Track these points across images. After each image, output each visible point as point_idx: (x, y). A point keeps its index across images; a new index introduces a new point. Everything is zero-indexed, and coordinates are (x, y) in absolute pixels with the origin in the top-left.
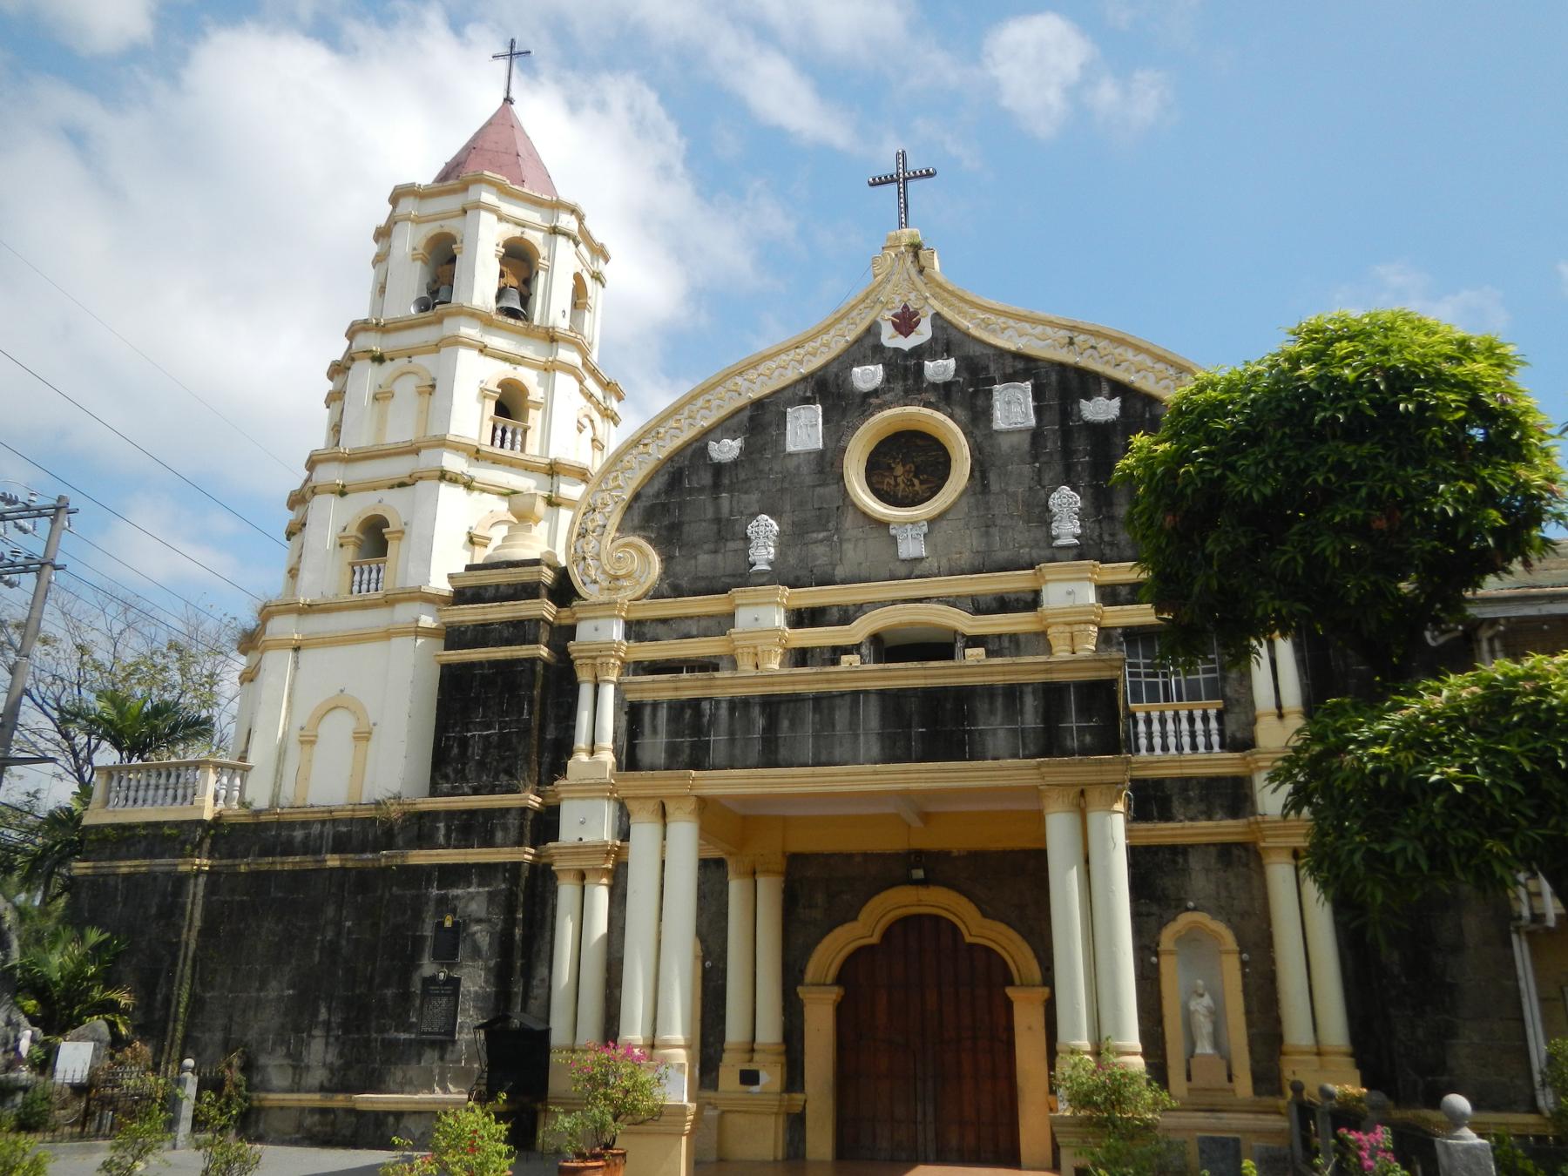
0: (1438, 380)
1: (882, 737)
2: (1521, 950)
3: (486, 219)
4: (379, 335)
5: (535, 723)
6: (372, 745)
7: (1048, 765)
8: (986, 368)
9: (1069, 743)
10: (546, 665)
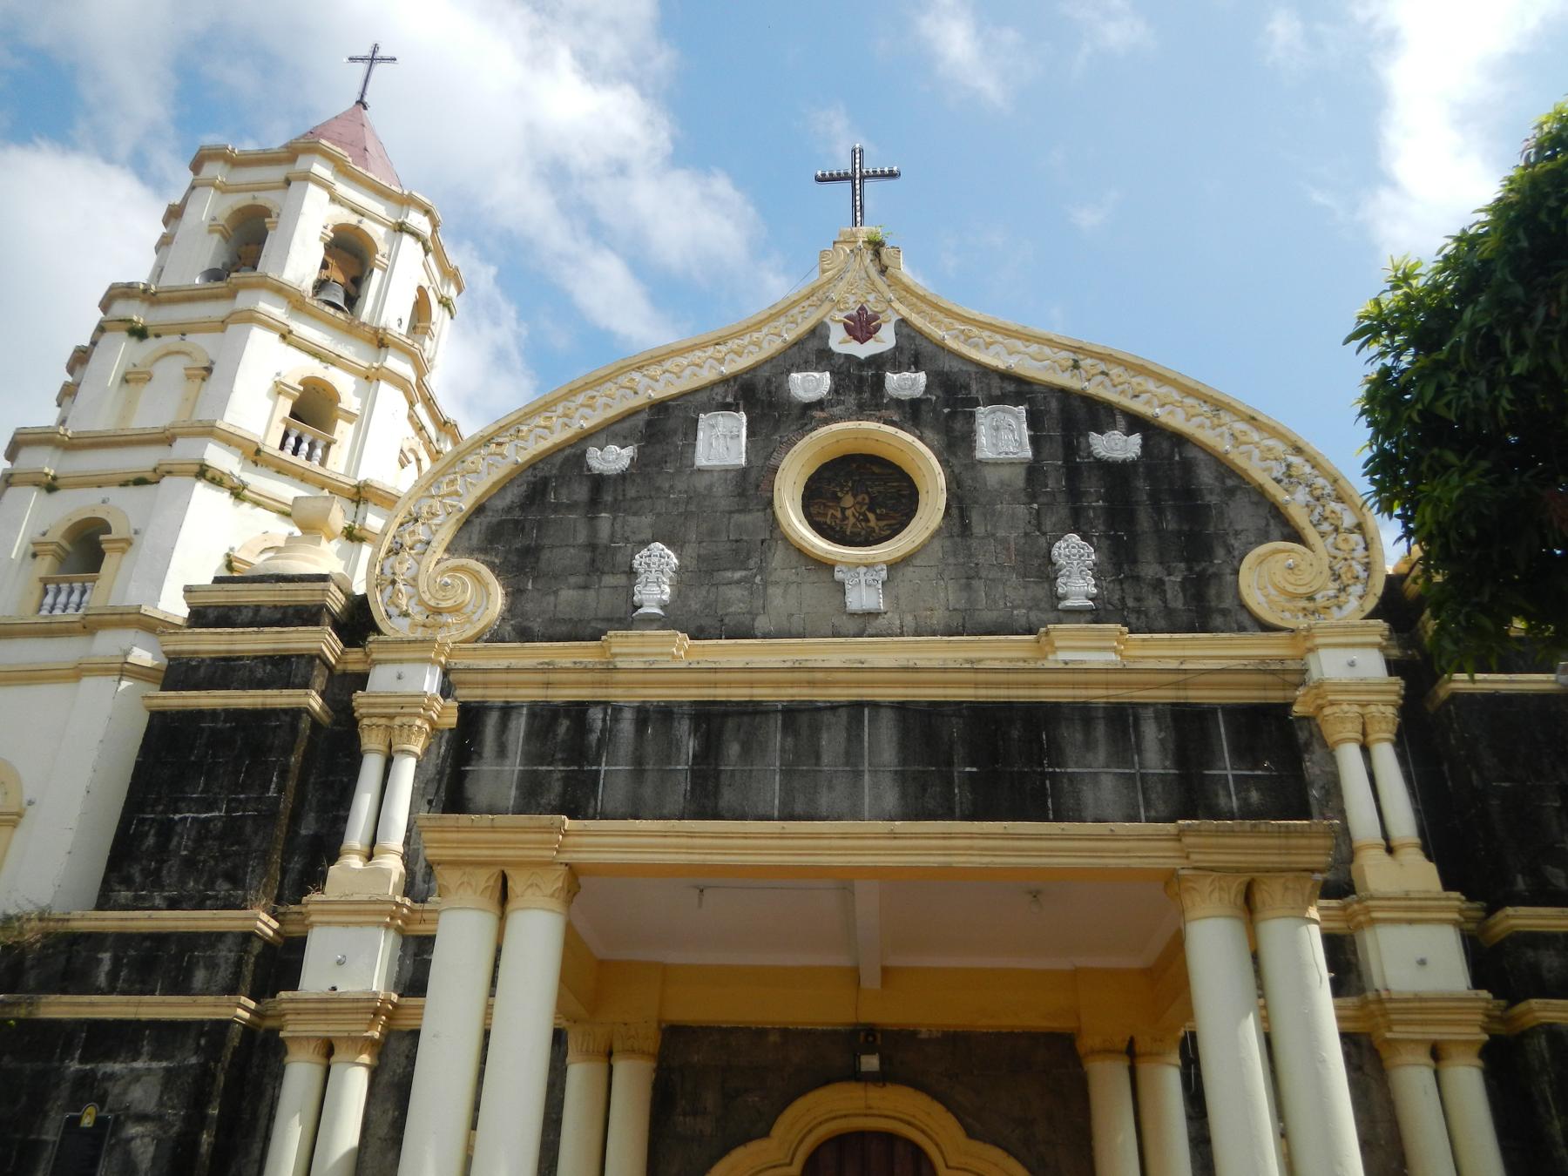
1: (902, 777)
5: (286, 805)
7: (1197, 832)
8: (967, 387)
9: (1222, 801)
10: (316, 724)
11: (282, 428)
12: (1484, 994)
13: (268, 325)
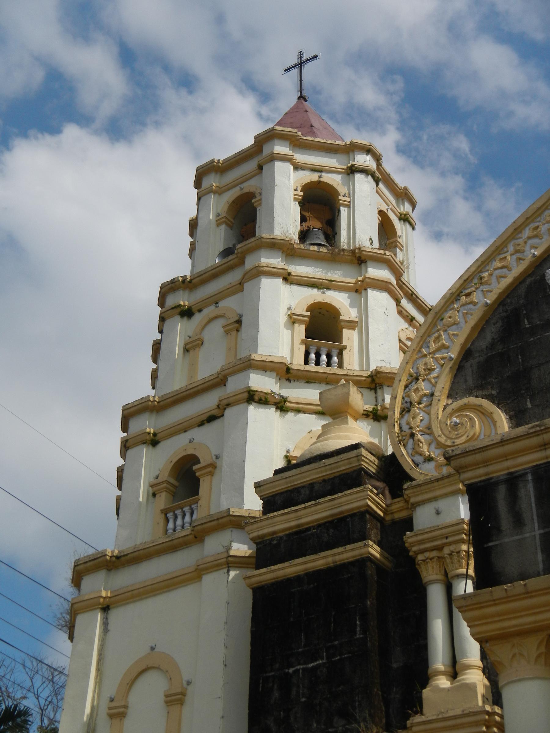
4: (187, 293)
6: (186, 710)
11: (303, 348)
13: (272, 274)
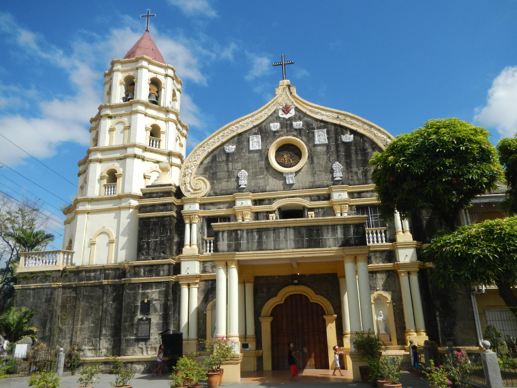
0: (470, 141)
2: (474, 299)
3: (145, 71)
8: (312, 125)
9: (351, 242)
12: (419, 261)
